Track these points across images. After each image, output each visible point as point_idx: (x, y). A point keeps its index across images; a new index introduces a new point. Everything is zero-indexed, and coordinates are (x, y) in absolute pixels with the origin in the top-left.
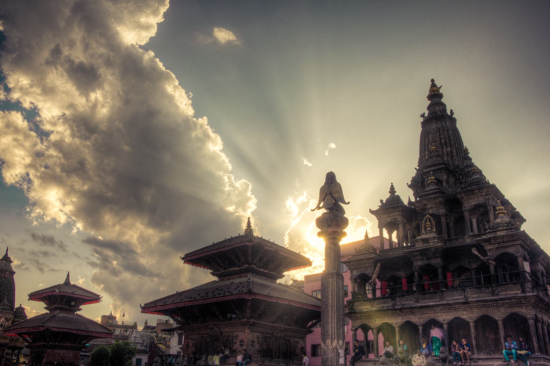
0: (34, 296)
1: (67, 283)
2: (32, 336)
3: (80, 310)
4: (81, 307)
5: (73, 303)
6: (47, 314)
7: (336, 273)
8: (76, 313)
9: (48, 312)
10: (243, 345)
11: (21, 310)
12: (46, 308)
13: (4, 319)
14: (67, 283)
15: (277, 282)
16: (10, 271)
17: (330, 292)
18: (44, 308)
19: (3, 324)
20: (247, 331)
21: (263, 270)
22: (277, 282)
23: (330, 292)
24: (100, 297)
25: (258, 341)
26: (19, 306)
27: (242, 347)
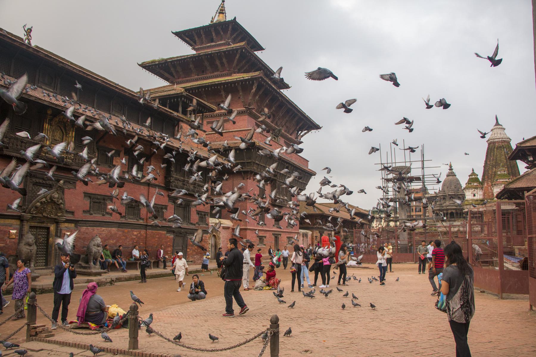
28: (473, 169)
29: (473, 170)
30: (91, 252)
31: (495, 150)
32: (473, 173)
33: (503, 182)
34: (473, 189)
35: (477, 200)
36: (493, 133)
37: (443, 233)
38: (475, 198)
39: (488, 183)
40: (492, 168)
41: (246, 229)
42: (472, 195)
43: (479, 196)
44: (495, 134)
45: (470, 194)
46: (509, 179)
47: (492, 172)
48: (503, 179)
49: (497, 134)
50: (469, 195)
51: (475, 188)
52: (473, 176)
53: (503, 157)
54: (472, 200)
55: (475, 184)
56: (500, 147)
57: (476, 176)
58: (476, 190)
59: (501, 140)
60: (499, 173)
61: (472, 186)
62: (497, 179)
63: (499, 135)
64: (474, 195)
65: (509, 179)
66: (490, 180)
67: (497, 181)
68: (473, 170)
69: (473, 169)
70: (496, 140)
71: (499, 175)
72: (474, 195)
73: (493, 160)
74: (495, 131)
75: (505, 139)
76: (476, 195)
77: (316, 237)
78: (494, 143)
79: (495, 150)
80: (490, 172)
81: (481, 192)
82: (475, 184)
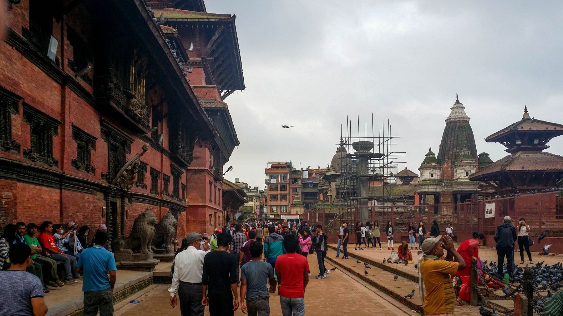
1: (526, 119)
2: (497, 182)
4: (547, 144)
5: (536, 142)
6: (509, 156)
8: (543, 151)
9: (511, 154)
12: (506, 151)
14: (526, 119)
18: (505, 151)
28: (430, 148)
29: (430, 149)
30: (169, 233)
31: (457, 129)
32: (430, 153)
33: (467, 163)
34: (432, 169)
35: (435, 181)
36: (454, 112)
37: (378, 214)
38: (432, 178)
39: (448, 164)
40: (453, 148)
41: (205, 207)
42: (430, 175)
43: (436, 176)
44: (456, 113)
45: (428, 174)
46: (473, 161)
47: (453, 152)
48: (467, 160)
49: (458, 112)
51: (434, 168)
52: (431, 156)
53: (464, 138)
54: (430, 180)
55: (434, 164)
56: (462, 127)
57: (433, 156)
58: (434, 170)
59: (462, 119)
60: (463, 154)
61: (430, 166)
62: (462, 160)
63: (460, 114)
64: (432, 176)
65: (473, 161)
66: (450, 161)
67: (461, 162)
68: (430, 149)
69: (430, 148)
70: (458, 119)
71: (463, 156)
72: (432, 176)
73: (454, 140)
74: (456, 110)
75: (466, 119)
76: (434, 175)
77: (219, 217)
78: (455, 122)
79: (457, 129)
80: (451, 152)
81: (439, 172)
82: (434, 164)
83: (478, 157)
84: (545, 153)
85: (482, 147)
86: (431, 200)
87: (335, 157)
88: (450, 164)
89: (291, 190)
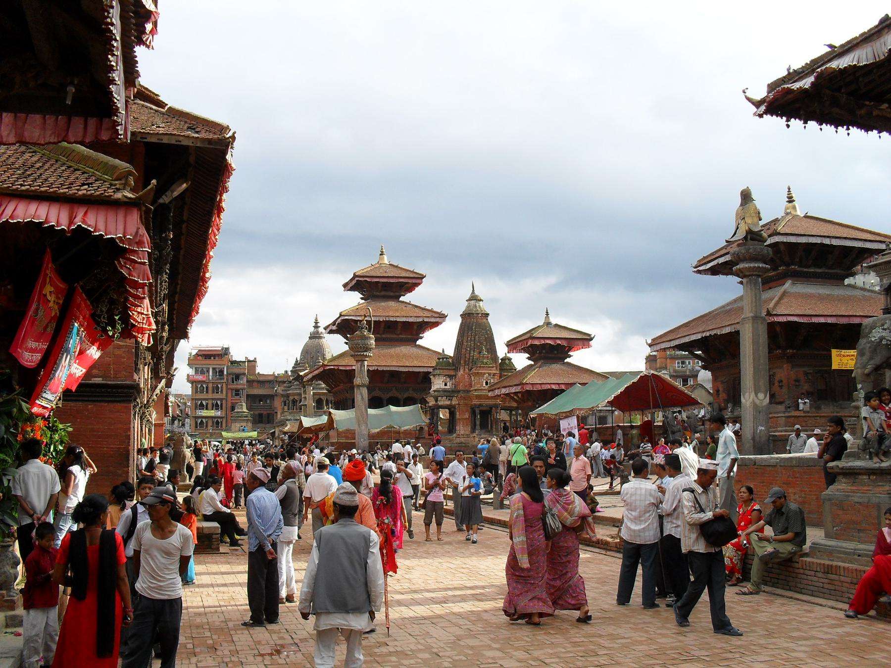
0: (513, 345)
3: (570, 356)
4: (571, 353)
7: (752, 317)
8: (566, 361)
9: (533, 363)
10: (782, 386)
11: (506, 361)
12: (529, 358)
13: (487, 375)
15: (846, 284)
16: (482, 314)
17: (747, 339)
19: (489, 381)
20: (785, 366)
21: (813, 270)
22: (846, 284)
23: (747, 339)
24: (592, 336)
25: (806, 378)
26: (504, 355)
27: (781, 389)
38: (446, 387)
39: (465, 370)
42: (444, 383)
45: (441, 383)
50: (438, 384)
64: (446, 385)
72: (446, 385)
76: (448, 384)
83: (500, 361)
84: (567, 362)
85: (502, 351)
86: (443, 414)
87: (306, 345)
88: (467, 370)
89: (230, 392)
